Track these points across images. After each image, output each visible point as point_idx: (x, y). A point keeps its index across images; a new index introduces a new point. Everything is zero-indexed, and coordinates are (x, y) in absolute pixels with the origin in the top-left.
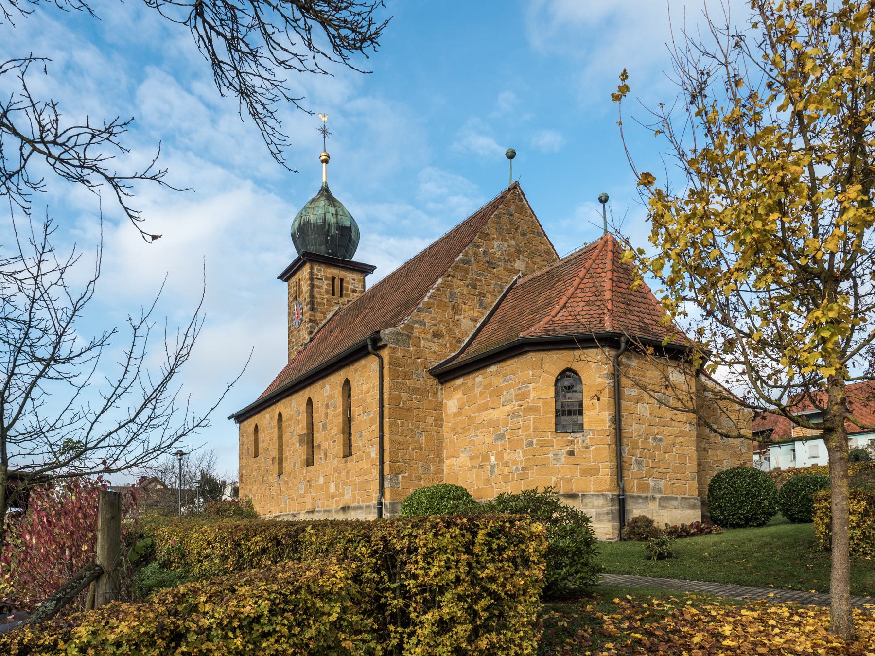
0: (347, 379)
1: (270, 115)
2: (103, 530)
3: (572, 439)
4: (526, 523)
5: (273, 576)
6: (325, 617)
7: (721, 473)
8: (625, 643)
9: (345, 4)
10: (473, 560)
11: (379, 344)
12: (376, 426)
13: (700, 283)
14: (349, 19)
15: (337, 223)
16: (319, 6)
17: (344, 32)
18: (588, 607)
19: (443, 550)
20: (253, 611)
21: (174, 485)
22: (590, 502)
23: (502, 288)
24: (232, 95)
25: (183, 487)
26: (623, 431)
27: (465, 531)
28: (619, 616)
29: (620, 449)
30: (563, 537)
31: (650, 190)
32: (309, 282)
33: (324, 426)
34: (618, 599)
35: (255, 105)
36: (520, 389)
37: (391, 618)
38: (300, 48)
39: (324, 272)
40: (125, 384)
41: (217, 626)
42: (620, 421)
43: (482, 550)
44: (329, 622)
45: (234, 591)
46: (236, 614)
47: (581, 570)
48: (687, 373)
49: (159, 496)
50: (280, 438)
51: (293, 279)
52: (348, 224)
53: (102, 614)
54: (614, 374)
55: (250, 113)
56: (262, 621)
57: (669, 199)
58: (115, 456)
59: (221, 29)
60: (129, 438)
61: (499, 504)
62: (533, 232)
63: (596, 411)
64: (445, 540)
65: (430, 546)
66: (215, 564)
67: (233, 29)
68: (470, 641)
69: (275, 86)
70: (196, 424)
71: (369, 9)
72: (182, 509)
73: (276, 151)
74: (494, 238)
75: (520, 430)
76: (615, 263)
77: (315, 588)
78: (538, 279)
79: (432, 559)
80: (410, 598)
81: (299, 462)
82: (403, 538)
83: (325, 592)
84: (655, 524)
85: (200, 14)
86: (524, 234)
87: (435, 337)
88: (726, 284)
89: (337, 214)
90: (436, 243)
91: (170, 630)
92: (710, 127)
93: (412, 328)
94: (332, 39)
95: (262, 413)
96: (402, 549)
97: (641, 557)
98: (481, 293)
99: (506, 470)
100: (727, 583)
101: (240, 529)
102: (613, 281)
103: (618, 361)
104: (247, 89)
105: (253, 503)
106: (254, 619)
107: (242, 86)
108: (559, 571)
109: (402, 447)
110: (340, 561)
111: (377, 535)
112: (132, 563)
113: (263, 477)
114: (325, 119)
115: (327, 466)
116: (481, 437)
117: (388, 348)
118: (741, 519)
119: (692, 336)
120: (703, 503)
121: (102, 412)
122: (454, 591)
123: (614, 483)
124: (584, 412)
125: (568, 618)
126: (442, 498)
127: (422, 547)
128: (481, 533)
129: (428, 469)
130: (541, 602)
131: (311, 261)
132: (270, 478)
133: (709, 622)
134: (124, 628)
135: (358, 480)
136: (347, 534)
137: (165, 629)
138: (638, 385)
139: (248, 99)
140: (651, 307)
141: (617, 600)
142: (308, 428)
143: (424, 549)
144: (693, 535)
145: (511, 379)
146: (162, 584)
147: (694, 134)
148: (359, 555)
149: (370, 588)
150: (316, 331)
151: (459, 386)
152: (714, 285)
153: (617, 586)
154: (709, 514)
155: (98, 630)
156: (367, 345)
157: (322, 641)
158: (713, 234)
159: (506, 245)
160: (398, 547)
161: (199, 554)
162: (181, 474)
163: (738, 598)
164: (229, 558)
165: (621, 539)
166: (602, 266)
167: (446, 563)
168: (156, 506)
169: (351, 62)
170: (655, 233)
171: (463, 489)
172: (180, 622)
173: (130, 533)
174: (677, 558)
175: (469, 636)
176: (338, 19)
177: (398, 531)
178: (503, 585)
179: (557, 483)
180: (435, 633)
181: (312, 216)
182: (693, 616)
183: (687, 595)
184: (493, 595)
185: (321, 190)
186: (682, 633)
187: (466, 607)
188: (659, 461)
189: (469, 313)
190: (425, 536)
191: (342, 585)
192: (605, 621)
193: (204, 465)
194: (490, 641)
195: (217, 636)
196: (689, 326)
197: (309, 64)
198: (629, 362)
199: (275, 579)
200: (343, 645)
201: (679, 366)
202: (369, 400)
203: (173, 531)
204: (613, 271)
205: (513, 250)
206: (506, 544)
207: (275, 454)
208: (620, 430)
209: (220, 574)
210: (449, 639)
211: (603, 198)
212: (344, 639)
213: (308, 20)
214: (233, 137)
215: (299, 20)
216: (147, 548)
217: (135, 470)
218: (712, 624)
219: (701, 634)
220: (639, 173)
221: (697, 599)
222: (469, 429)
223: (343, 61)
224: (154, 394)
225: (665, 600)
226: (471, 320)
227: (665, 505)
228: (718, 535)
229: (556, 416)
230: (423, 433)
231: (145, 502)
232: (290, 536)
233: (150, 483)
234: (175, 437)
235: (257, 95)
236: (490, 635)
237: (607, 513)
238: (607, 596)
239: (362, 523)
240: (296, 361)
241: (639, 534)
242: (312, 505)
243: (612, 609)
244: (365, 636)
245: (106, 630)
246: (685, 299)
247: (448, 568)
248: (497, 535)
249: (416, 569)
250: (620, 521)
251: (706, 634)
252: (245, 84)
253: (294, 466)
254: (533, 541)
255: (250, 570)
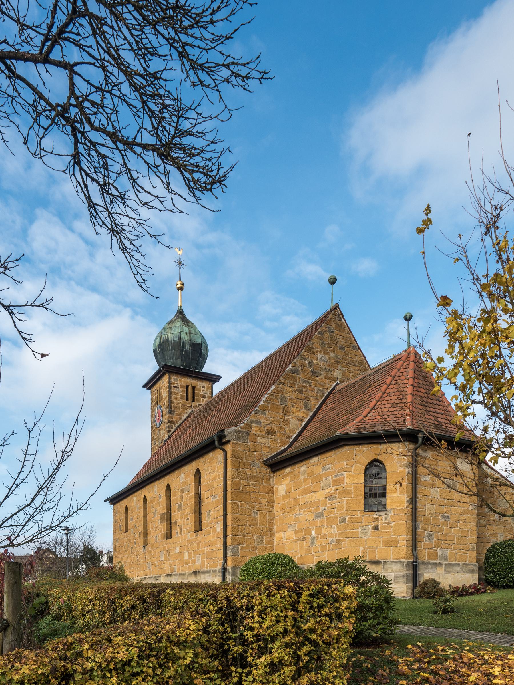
0: (198, 469)
1: (136, 249)
2: (8, 592)
3: (377, 516)
4: (340, 586)
5: (141, 629)
6: (181, 661)
7: (496, 544)
8: (416, 681)
9: (198, 151)
10: (297, 616)
11: (224, 440)
12: (221, 507)
13: (487, 388)
14: (201, 164)
15: (190, 340)
16: (176, 153)
17: (196, 176)
18: (387, 652)
19: (274, 608)
20: (125, 656)
21: (63, 554)
22: (390, 568)
23: (324, 393)
24: (104, 232)
25: (69, 556)
26: (418, 510)
27: (292, 593)
28: (411, 659)
29: (415, 525)
30: (369, 596)
31: (447, 310)
32: (168, 390)
33: (180, 507)
34: (410, 645)
35: (124, 241)
36: (336, 476)
37: (232, 661)
38: (161, 190)
39: (180, 382)
40: (23, 475)
41: (97, 668)
42: (416, 502)
43: (305, 608)
44: (184, 665)
45: (110, 640)
46: (112, 659)
47: (382, 622)
48: (474, 464)
49: (51, 563)
50: (145, 516)
51: (155, 388)
52: (199, 341)
53: (8, 659)
54: (412, 464)
55: (120, 248)
56: (132, 664)
57: (465, 317)
58: (16, 534)
59: (94, 176)
60: (27, 520)
61: (318, 570)
62: (349, 346)
63: (397, 494)
64: (276, 600)
65: (264, 604)
66: (95, 617)
67: (105, 176)
68: (294, 679)
69: (140, 224)
70: (79, 508)
71: (218, 155)
72: (69, 573)
73: (141, 280)
74: (317, 352)
75: (335, 510)
76: (416, 372)
77: (173, 638)
78: (353, 385)
79: (266, 615)
80: (247, 645)
81: (160, 536)
82: (243, 598)
83: (181, 641)
84: (441, 586)
85: (77, 162)
86: (342, 348)
87: (268, 434)
88: (508, 390)
89: (190, 333)
90: (270, 356)
91: (61, 672)
92: (501, 254)
93: (250, 427)
94: (187, 182)
95: (131, 496)
96: (242, 606)
97: (429, 611)
98: (306, 397)
99: (324, 542)
100: (497, 633)
101: (115, 590)
102: (414, 387)
103: (416, 453)
104: (117, 227)
105: (124, 568)
106: (126, 663)
107: (113, 224)
108: (364, 623)
109: (242, 523)
110: (193, 616)
111: (222, 595)
112: (31, 617)
113: (132, 548)
114: (180, 253)
115: (182, 539)
116: (304, 515)
117: (231, 443)
118: (510, 581)
119: (478, 433)
120: (480, 569)
121: (5, 499)
122: (282, 640)
123: (410, 552)
124: (387, 495)
125: (371, 661)
126: (273, 564)
127: (257, 606)
128: (305, 594)
129: (262, 541)
130: (350, 649)
131: (169, 372)
132: (138, 548)
133: (482, 664)
134: (25, 670)
135: (206, 550)
136: (198, 594)
137: (57, 671)
138: (433, 473)
139: (118, 236)
140: (445, 408)
141: (410, 646)
142: (167, 509)
143: (260, 607)
144: (471, 594)
145: (329, 468)
146: (54, 633)
147: (487, 261)
148: (208, 611)
149: (216, 637)
150: (173, 430)
151: (287, 475)
152: (498, 390)
153: (410, 635)
154: (484, 577)
155: (6, 672)
156: (214, 441)
157: (179, 679)
158: (499, 347)
159: (327, 357)
160: (239, 606)
161: (83, 609)
162: (68, 545)
163: (506, 645)
164: (106, 613)
165: (414, 597)
166: (405, 374)
167: (276, 618)
168: (49, 570)
169: (203, 202)
170: (451, 347)
171: (289, 557)
172: (69, 666)
173: (29, 593)
174: (458, 613)
175: (294, 675)
176: (192, 164)
177: (239, 593)
178: (321, 636)
179: (364, 552)
180: (266, 673)
181: (170, 335)
182: (470, 659)
183: (465, 642)
184: (313, 643)
185: (177, 313)
186: (461, 673)
187: (291, 653)
188: (446, 534)
189: (297, 414)
190: (260, 597)
191: (195, 635)
192: (400, 663)
193: (86, 538)
194: (310, 679)
195: (98, 675)
196: (476, 424)
197: (168, 204)
198: (425, 454)
199: (142, 631)
200: (195, 682)
201: (467, 458)
202: (215, 486)
203: (62, 591)
204: (414, 378)
205: (332, 361)
206: (324, 603)
207: (141, 529)
208: (416, 509)
209: (100, 625)
210: (278, 677)
211: (408, 317)
212: (196, 678)
213: (167, 166)
214: (107, 268)
215: (160, 166)
216: (43, 604)
217: (32, 544)
218: (485, 666)
219: (476, 674)
220: (439, 296)
221: (473, 646)
222: (295, 509)
223: (196, 201)
224: (46, 484)
225: (447, 646)
226: (298, 420)
227: (449, 570)
228: (491, 594)
229: (365, 498)
230: (258, 512)
231: (40, 568)
232: (153, 595)
233: (45, 552)
234: (63, 518)
235: (126, 232)
236: (310, 674)
237: (403, 576)
238: (402, 643)
239: (210, 586)
240: (158, 454)
241: (428, 593)
242: (171, 569)
243: (406, 653)
244: (212, 675)
245: (12, 672)
246: (474, 402)
247: (278, 622)
248: (317, 595)
249: (252, 623)
250: (413, 582)
251: (480, 674)
252: (115, 223)
253: (156, 539)
254: (345, 600)
255: (122, 623)
